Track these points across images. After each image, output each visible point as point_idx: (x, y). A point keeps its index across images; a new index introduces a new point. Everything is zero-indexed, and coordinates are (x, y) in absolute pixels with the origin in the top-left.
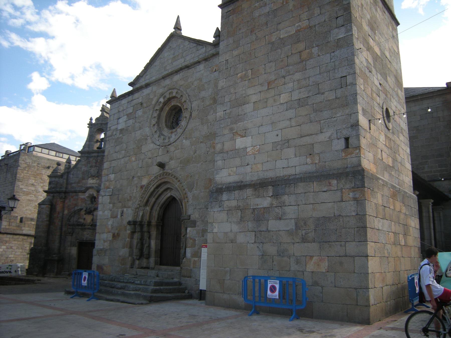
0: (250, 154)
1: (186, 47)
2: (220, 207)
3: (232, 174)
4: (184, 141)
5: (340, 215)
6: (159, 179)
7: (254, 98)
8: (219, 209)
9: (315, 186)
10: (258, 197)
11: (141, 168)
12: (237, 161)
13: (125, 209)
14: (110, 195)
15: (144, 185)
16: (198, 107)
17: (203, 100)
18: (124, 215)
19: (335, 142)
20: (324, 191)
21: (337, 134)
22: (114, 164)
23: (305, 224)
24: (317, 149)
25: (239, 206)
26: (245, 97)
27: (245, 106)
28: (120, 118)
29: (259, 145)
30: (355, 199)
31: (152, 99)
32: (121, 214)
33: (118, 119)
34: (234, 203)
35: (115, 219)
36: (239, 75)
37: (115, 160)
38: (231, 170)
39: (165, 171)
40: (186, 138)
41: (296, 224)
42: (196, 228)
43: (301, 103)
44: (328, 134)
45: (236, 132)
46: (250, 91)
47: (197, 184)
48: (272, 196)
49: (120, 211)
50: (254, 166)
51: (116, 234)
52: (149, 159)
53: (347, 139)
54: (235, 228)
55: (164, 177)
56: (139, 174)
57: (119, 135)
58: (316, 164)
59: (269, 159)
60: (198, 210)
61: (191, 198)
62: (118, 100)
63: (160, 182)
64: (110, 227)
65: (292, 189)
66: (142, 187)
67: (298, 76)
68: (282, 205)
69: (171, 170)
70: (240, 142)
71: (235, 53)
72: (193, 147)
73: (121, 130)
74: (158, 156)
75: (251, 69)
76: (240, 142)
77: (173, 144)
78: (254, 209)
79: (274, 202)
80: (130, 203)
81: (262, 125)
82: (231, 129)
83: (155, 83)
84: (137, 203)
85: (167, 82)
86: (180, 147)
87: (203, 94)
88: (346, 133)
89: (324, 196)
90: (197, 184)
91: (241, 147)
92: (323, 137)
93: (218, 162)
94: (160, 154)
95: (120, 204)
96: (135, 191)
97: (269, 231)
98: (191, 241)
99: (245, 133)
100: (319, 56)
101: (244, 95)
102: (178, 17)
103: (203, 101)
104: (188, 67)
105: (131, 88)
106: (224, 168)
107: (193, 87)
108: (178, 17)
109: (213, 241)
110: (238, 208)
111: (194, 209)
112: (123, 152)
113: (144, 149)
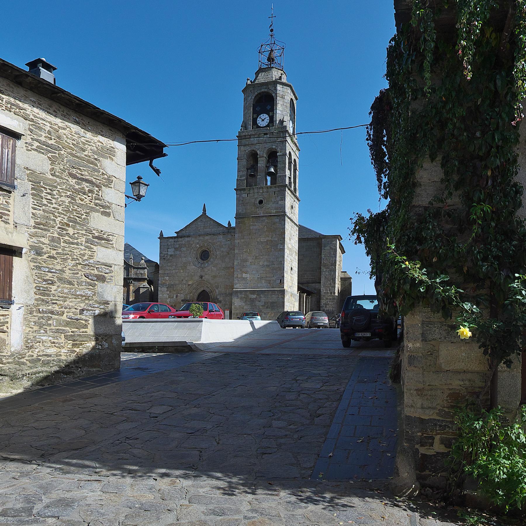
7: (250, 261)
17: (222, 252)
24: (272, 282)
31: (192, 244)
33: (168, 249)
36: (244, 250)
43: (268, 266)
44: (275, 278)
46: (249, 258)
51: (173, 305)
53: (281, 280)
54: (243, 304)
64: (168, 302)
66: (189, 285)
67: (266, 257)
70: (244, 275)
71: (242, 241)
73: (171, 255)
76: (244, 275)
82: (241, 270)
87: (222, 249)
88: (280, 278)
92: (274, 278)
96: (185, 286)
102: (204, 204)
105: (176, 235)
108: (204, 204)
110: (244, 297)
113: (188, 267)
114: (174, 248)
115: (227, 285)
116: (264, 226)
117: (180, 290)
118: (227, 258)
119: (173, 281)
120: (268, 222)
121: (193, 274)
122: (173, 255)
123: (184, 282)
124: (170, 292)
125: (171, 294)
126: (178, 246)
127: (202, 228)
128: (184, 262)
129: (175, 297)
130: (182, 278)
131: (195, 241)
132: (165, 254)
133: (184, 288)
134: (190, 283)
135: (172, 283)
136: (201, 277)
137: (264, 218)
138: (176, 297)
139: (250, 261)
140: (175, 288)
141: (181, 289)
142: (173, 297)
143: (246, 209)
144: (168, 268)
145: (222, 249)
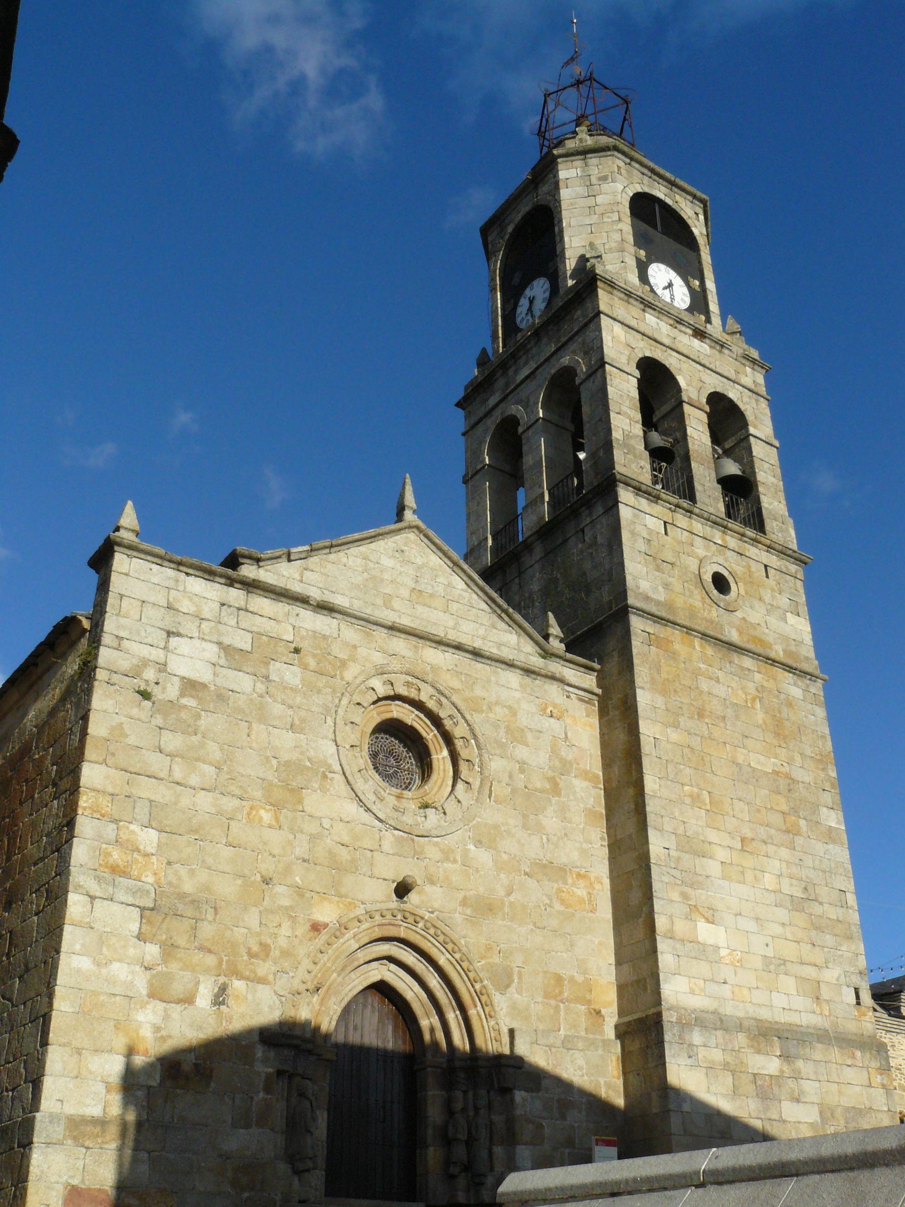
0: (727, 962)
1: (459, 592)
2: (690, 1057)
3: (697, 991)
4: (472, 847)
5: (871, 1108)
6: (377, 923)
8: (689, 1062)
9: (835, 1054)
10: (759, 1052)
11: (304, 861)
12: (703, 968)
13: (238, 985)
14: (143, 909)
15: (326, 925)
16: (510, 777)
18: (231, 1002)
19: (845, 989)
20: (849, 1066)
21: (845, 976)
22: (146, 789)
23: (832, 1114)
25: (728, 1063)
26: (703, 841)
27: (705, 860)
28: (179, 635)
29: (741, 952)
30: (884, 1086)
31: (343, 664)
32: (217, 996)
33: (169, 634)
34: (717, 1055)
35: (179, 1008)
37: (162, 779)
38: (696, 984)
39: (407, 907)
40: (480, 842)
41: (821, 1113)
42: (540, 1094)
45: (695, 906)
46: (712, 836)
47: (520, 978)
48: (780, 1056)
50: (736, 989)
52: (340, 845)
55: (396, 922)
56: (297, 879)
57: (182, 695)
58: (826, 1016)
59: (760, 985)
60: (544, 1048)
61: (504, 1010)
62: (166, 563)
65: (808, 1050)
66: (316, 927)
67: (784, 853)
68: (797, 1076)
69: (432, 913)
72: (502, 876)
73: (190, 686)
74: (377, 850)
75: (709, 792)
76: (705, 932)
77: (436, 839)
78: (755, 1075)
79: (785, 1069)
80: (264, 968)
81: (740, 914)
82: (685, 896)
83: (353, 621)
84: (301, 973)
85: (400, 644)
86: (459, 858)
87: (521, 752)
89: (850, 1074)
90: (520, 978)
91: (711, 941)
93: (665, 955)
94: (387, 846)
95: (211, 960)
96: (285, 930)
97: (784, 1121)
98: (531, 1126)
99: (713, 915)
100: (809, 836)
101: (702, 838)
103: (522, 771)
104: (476, 654)
106: (679, 974)
107: (491, 715)
109: (685, 1131)
110: (726, 1066)
111: (532, 1043)
112: (210, 770)
113: (313, 801)
114: (219, 644)
115: (559, 979)
116: (753, 700)
117: (251, 955)
118: (550, 811)
119: (192, 873)
120: (765, 684)
121: (344, 854)
122: (204, 686)
123: (282, 894)
124: (169, 950)
125: (174, 967)
126: (243, 641)
127: (405, 593)
128: (285, 757)
129: (204, 999)
130: (267, 866)
131: (362, 652)
132: (145, 663)
133: (282, 942)
134: (327, 913)
135: (188, 887)
136: (403, 890)
137: (748, 662)
139: (722, 854)
140: (207, 930)
141: (255, 948)
142: (188, 1000)
143: (667, 586)
144: (157, 763)
145: (521, 752)
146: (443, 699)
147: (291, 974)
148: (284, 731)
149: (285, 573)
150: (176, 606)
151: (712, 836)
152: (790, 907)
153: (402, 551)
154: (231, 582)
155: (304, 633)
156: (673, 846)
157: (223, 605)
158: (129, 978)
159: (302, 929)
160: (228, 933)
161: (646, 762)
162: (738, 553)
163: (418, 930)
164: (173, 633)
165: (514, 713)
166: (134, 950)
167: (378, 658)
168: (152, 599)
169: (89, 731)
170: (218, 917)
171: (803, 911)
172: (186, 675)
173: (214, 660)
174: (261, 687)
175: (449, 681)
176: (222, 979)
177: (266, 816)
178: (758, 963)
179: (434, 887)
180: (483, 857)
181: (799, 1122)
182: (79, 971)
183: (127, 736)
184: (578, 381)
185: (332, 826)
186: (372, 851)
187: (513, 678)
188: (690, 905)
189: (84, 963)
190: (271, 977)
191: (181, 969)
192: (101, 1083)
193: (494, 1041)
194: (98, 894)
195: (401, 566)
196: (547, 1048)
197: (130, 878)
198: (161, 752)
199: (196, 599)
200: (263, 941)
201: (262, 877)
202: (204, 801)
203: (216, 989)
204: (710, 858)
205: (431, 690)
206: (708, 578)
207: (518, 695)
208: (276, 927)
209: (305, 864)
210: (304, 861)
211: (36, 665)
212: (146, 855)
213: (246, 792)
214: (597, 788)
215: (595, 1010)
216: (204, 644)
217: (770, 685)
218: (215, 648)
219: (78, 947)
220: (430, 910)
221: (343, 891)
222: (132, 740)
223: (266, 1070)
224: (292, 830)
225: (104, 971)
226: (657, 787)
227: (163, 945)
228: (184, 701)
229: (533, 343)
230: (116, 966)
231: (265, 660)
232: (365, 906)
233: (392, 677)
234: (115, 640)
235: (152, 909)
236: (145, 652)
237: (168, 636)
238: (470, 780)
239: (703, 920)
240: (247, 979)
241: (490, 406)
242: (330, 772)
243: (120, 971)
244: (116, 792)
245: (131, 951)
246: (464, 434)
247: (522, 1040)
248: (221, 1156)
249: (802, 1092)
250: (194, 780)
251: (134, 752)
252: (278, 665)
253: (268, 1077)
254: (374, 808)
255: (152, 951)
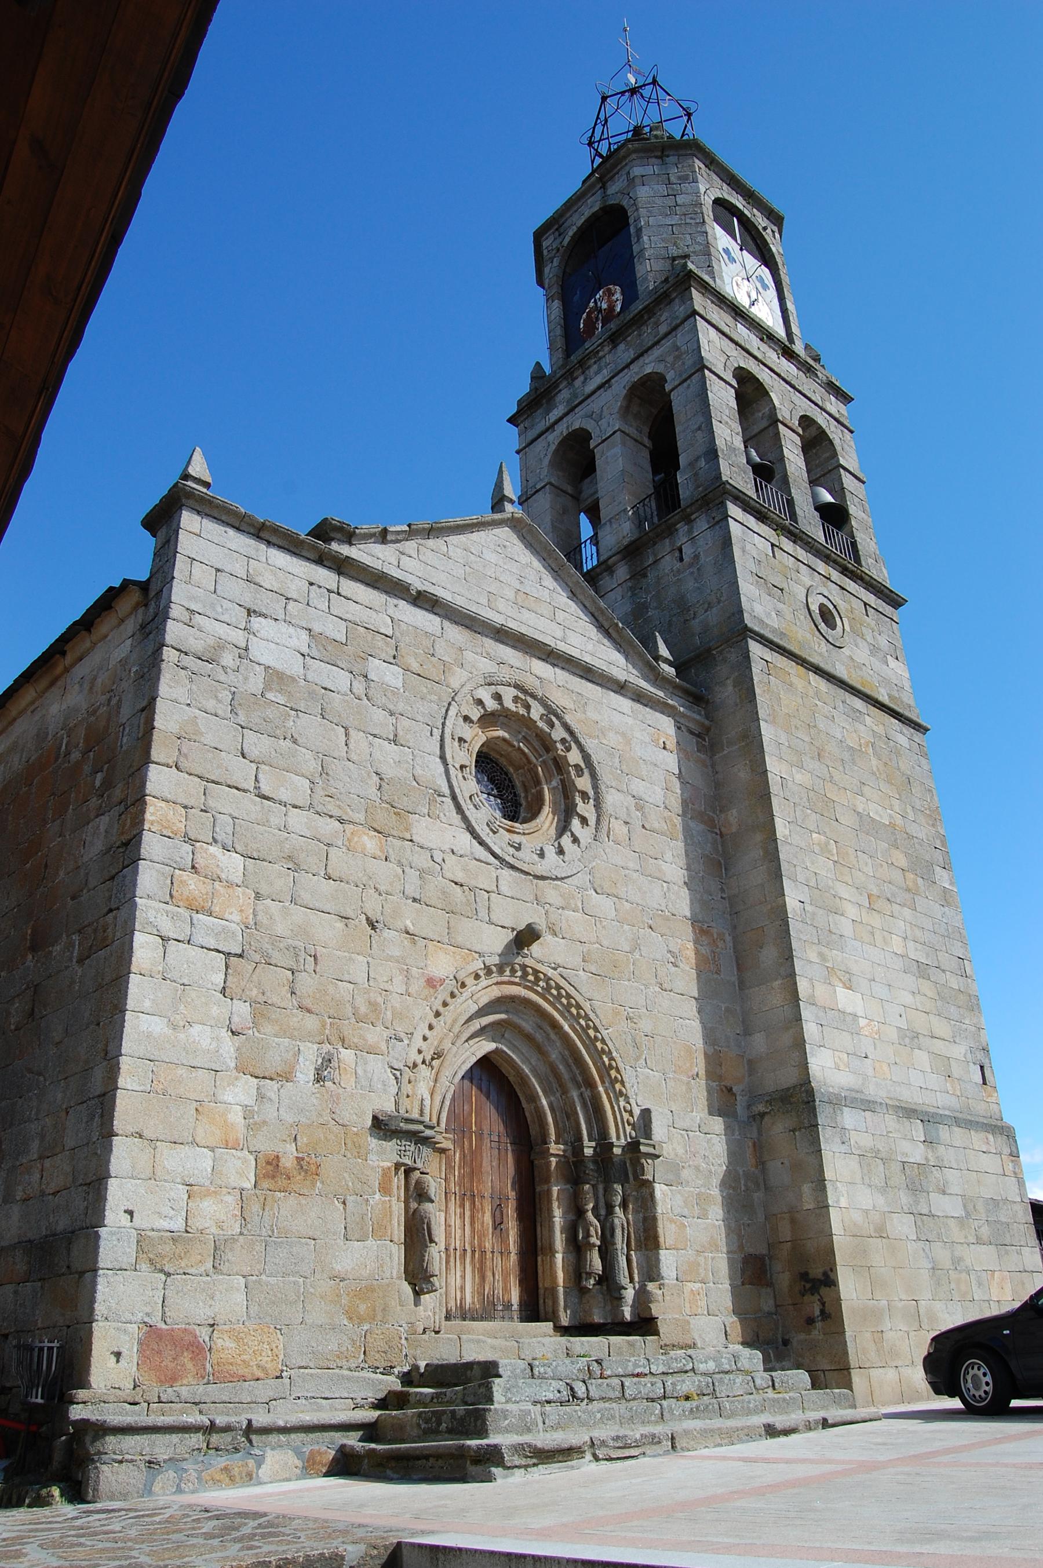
8: (844, 1148)
11: (415, 900)
15: (442, 981)
22: (223, 800)
27: (837, 917)
45: (833, 969)
49: (309, 1058)
51: (288, 1162)
56: (408, 923)
63: (496, 992)
64: (236, 1117)
66: (431, 983)
67: (907, 912)
69: (555, 969)
73: (275, 678)
76: (845, 998)
80: (375, 1035)
95: (311, 1023)
124: (261, 1009)
126: (336, 630)
127: (510, 594)
129: (305, 1073)
132: (221, 645)
138: (319, 1079)
140: (306, 983)
141: (363, 1009)
142: (286, 1076)
143: (778, 613)
146: (554, 719)
147: (406, 1042)
148: (386, 742)
149: (380, 556)
150: (258, 579)
151: (844, 891)
152: (917, 974)
153: (505, 547)
154: (321, 560)
155: (404, 626)
156: (807, 900)
157: (311, 584)
158: (214, 1045)
159: (417, 985)
160: (331, 989)
161: (775, 801)
162: (840, 586)
163: (539, 989)
164: (255, 611)
165: (628, 742)
166: (220, 1008)
167: (486, 666)
168: (228, 568)
169: (156, 724)
170: (318, 967)
171: (929, 979)
172: (272, 664)
173: (305, 650)
174: (359, 687)
175: (559, 699)
176: (326, 1047)
177: (370, 842)
178: (893, 1035)
179: (556, 939)
180: (603, 905)
181: (947, 1217)
182: (149, 1035)
183: (202, 734)
184: (668, 387)
185: (444, 860)
186: (488, 892)
187: (625, 704)
188: (827, 967)
189: (157, 1026)
190: (384, 1047)
191: (276, 1036)
192: (181, 1187)
193: (626, 1124)
194: (172, 935)
195: (505, 563)
196: (684, 1132)
197: (211, 915)
198: (244, 757)
199: (280, 574)
200: (372, 1000)
201: (368, 919)
202: (297, 820)
203: (320, 1061)
204: (842, 915)
205: (542, 711)
206: (815, 608)
207: (630, 721)
208: (387, 982)
209: (417, 905)
210: (415, 900)
211: (64, 653)
212: (230, 885)
213: (347, 813)
214: (712, 832)
215: (726, 1087)
216: (291, 630)
217: (880, 730)
218: (304, 635)
219: (147, 1004)
220: (553, 965)
221: (460, 940)
222: (209, 739)
223: (382, 1164)
224: (400, 864)
225: (182, 1036)
226: (787, 832)
227: (253, 1002)
228: (270, 695)
229: (607, 349)
230: (197, 1028)
231: (362, 654)
232: (483, 959)
233: (501, 689)
234: (186, 613)
235: (240, 956)
236: (222, 630)
237: (249, 615)
238: (586, 815)
239: (841, 985)
240: (357, 1048)
241: (552, 421)
242: (439, 795)
243: (201, 1035)
244: (190, 805)
245: (215, 1011)
246: (518, 452)
247: (659, 1123)
248: (333, 1278)
249: (946, 1183)
250: (284, 795)
251: (210, 755)
252: (377, 661)
253: (385, 1172)
254: (488, 841)
255: (242, 1011)
